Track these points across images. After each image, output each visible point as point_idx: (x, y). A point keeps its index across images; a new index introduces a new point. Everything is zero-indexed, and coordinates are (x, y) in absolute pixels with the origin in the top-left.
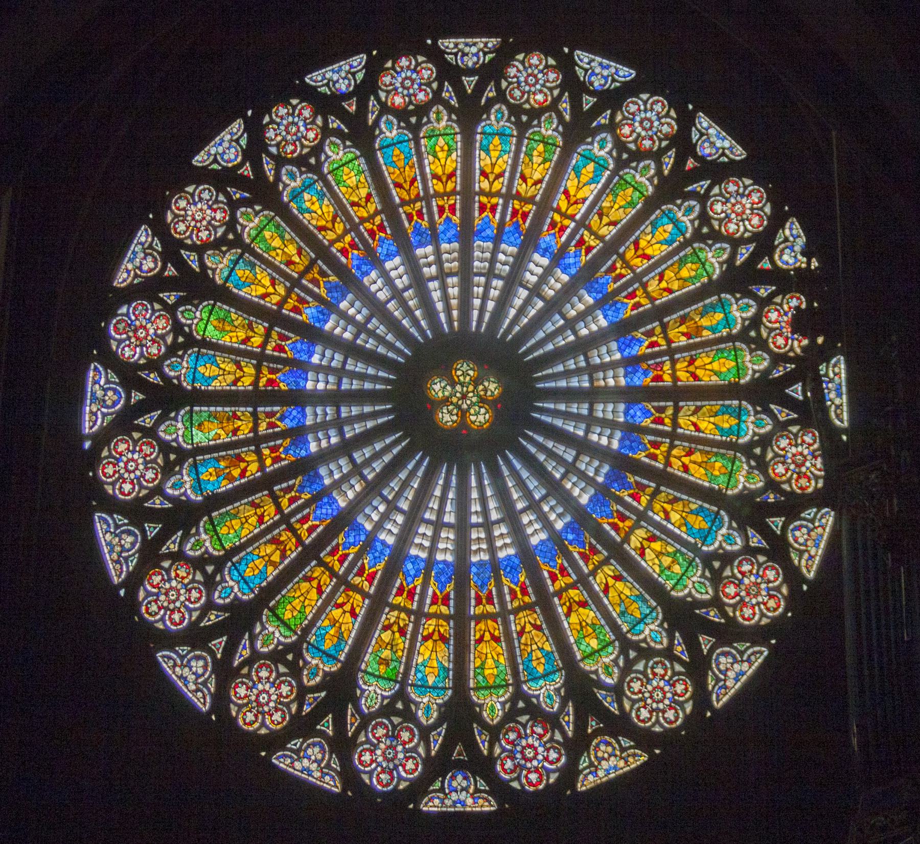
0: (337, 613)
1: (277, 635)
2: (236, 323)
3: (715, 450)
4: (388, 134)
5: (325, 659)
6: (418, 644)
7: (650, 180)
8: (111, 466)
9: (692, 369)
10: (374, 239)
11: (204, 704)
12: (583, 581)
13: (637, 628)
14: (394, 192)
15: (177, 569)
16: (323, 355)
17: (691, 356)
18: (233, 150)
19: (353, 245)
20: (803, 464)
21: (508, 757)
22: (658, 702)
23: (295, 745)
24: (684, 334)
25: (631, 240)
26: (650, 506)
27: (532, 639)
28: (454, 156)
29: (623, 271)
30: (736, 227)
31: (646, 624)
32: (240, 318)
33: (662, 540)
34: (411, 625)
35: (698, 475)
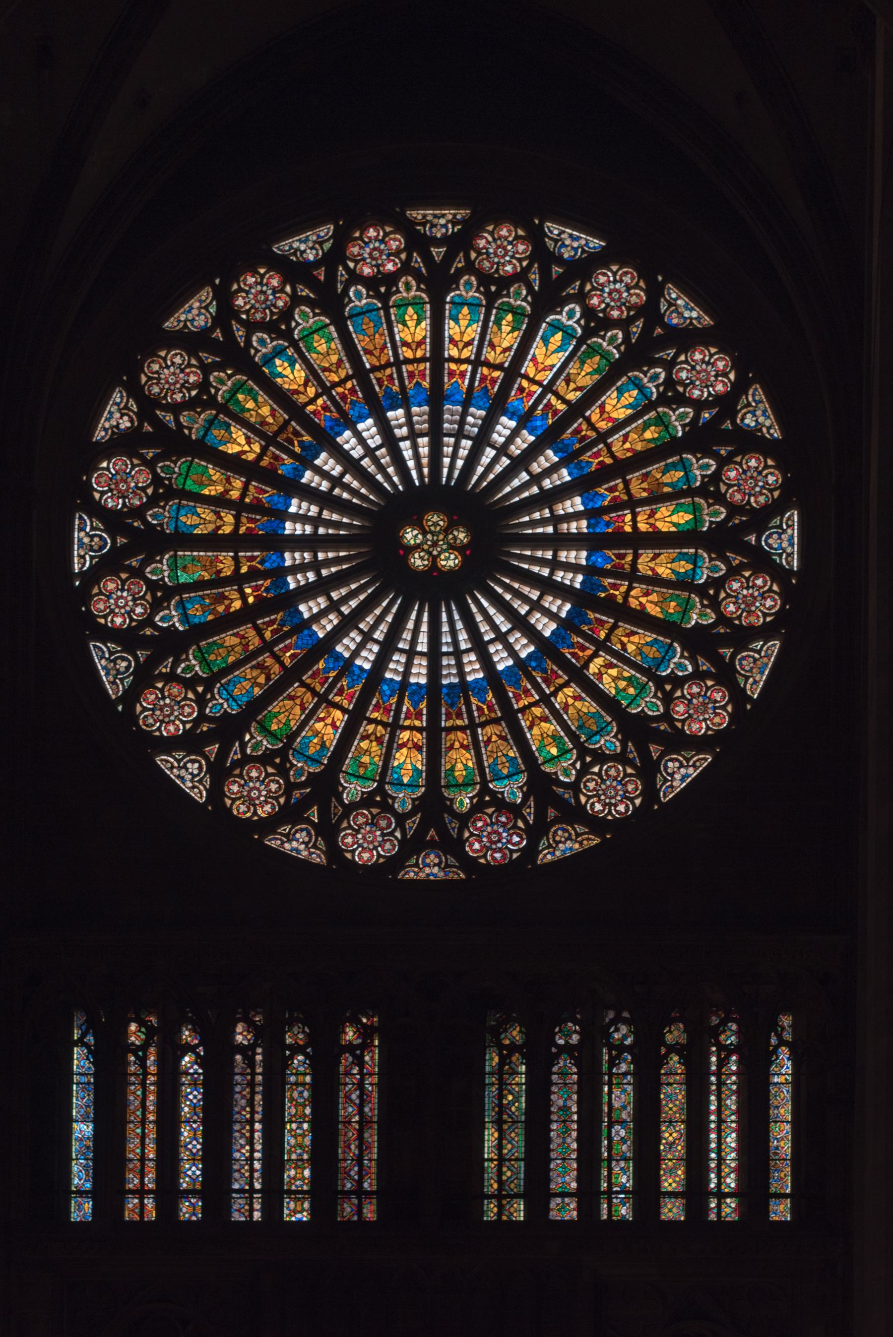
0: (319, 726)
1: (265, 743)
2: (214, 478)
3: (670, 591)
4: (357, 303)
5: (310, 763)
6: (394, 751)
7: (617, 348)
8: (102, 603)
9: (652, 521)
10: (346, 403)
11: (201, 797)
12: (545, 700)
13: (594, 739)
14: (364, 358)
15: (170, 689)
16: (300, 507)
17: (652, 510)
18: (203, 317)
19: (325, 408)
20: (753, 604)
21: (476, 840)
22: (611, 798)
23: (285, 830)
24: (644, 490)
25: (597, 404)
26: (608, 637)
27: (498, 747)
28: (423, 325)
29: (589, 433)
30: (700, 393)
31: (602, 736)
32: (218, 474)
33: (618, 667)
34: (387, 736)
35: (654, 610)
